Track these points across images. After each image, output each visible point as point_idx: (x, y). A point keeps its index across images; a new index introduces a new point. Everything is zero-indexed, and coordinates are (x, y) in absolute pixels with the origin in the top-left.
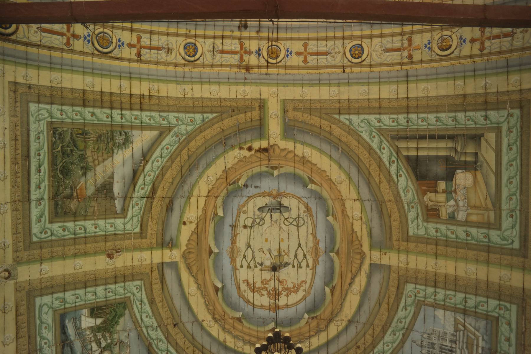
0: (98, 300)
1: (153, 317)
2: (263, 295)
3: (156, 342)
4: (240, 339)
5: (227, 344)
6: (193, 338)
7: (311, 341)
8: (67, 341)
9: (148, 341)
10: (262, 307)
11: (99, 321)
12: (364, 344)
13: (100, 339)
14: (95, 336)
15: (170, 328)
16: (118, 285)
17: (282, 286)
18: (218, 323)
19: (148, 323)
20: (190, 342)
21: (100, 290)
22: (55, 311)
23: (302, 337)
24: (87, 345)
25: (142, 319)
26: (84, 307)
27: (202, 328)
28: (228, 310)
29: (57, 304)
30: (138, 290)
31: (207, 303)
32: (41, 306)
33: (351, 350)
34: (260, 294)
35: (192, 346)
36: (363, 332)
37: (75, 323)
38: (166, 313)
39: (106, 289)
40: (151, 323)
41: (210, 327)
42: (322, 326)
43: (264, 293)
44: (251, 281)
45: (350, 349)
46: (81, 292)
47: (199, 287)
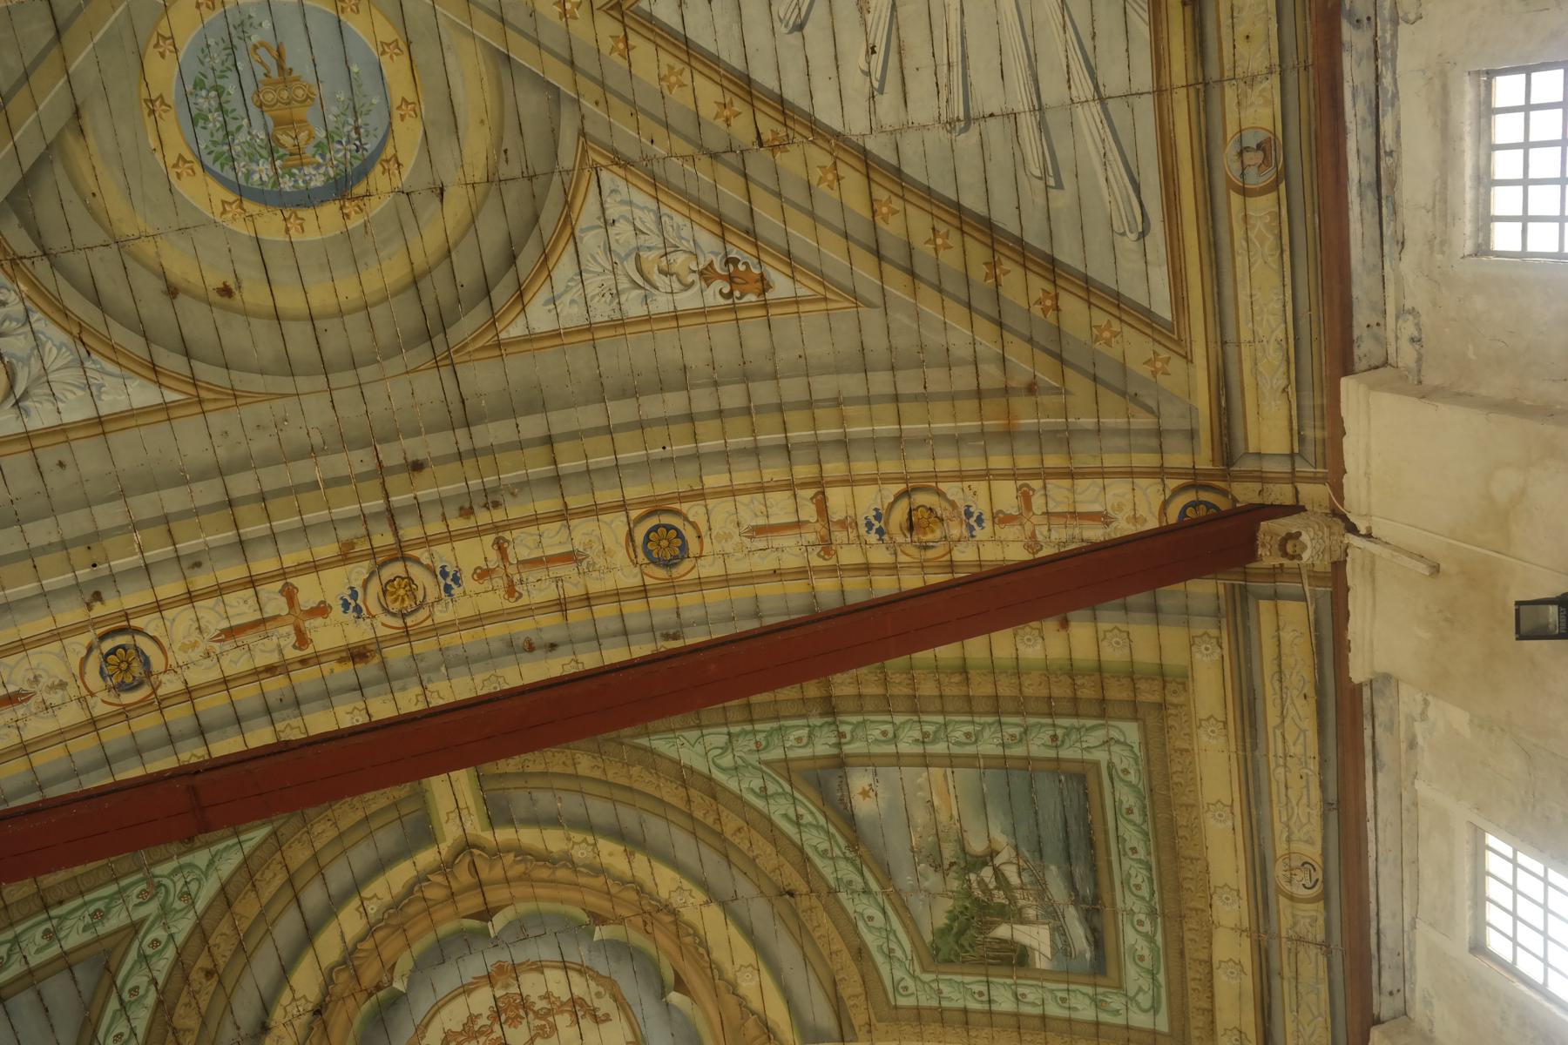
0: (1009, 981)
1: (852, 916)
2: (542, 998)
3: (837, 852)
4: (584, 866)
5: (622, 848)
6: (727, 857)
7: (364, 921)
8: (1087, 910)
9: (860, 856)
10: (539, 967)
11: (1003, 931)
12: (194, 994)
13: (996, 888)
14: (1013, 900)
15: (800, 885)
16: (960, 1004)
17: (494, 1036)
18: (659, 902)
19: (865, 901)
20: (732, 845)
21: (1005, 1003)
22: (1120, 987)
23: (394, 922)
24: (1032, 883)
25: (884, 913)
26: (1043, 975)
27: (704, 885)
28: (637, 939)
29: (1116, 1002)
30: (902, 984)
31: (702, 950)
32: (1155, 1009)
33: (228, 954)
34: (552, 999)
35: (728, 835)
36: (212, 1026)
37: (1066, 942)
38: (815, 924)
39: (990, 1001)
40: (856, 901)
41: (680, 888)
42: (343, 978)
43: (540, 1005)
44: (586, 1023)
45: (233, 956)
46: (1054, 1010)
47: (733, 989)
